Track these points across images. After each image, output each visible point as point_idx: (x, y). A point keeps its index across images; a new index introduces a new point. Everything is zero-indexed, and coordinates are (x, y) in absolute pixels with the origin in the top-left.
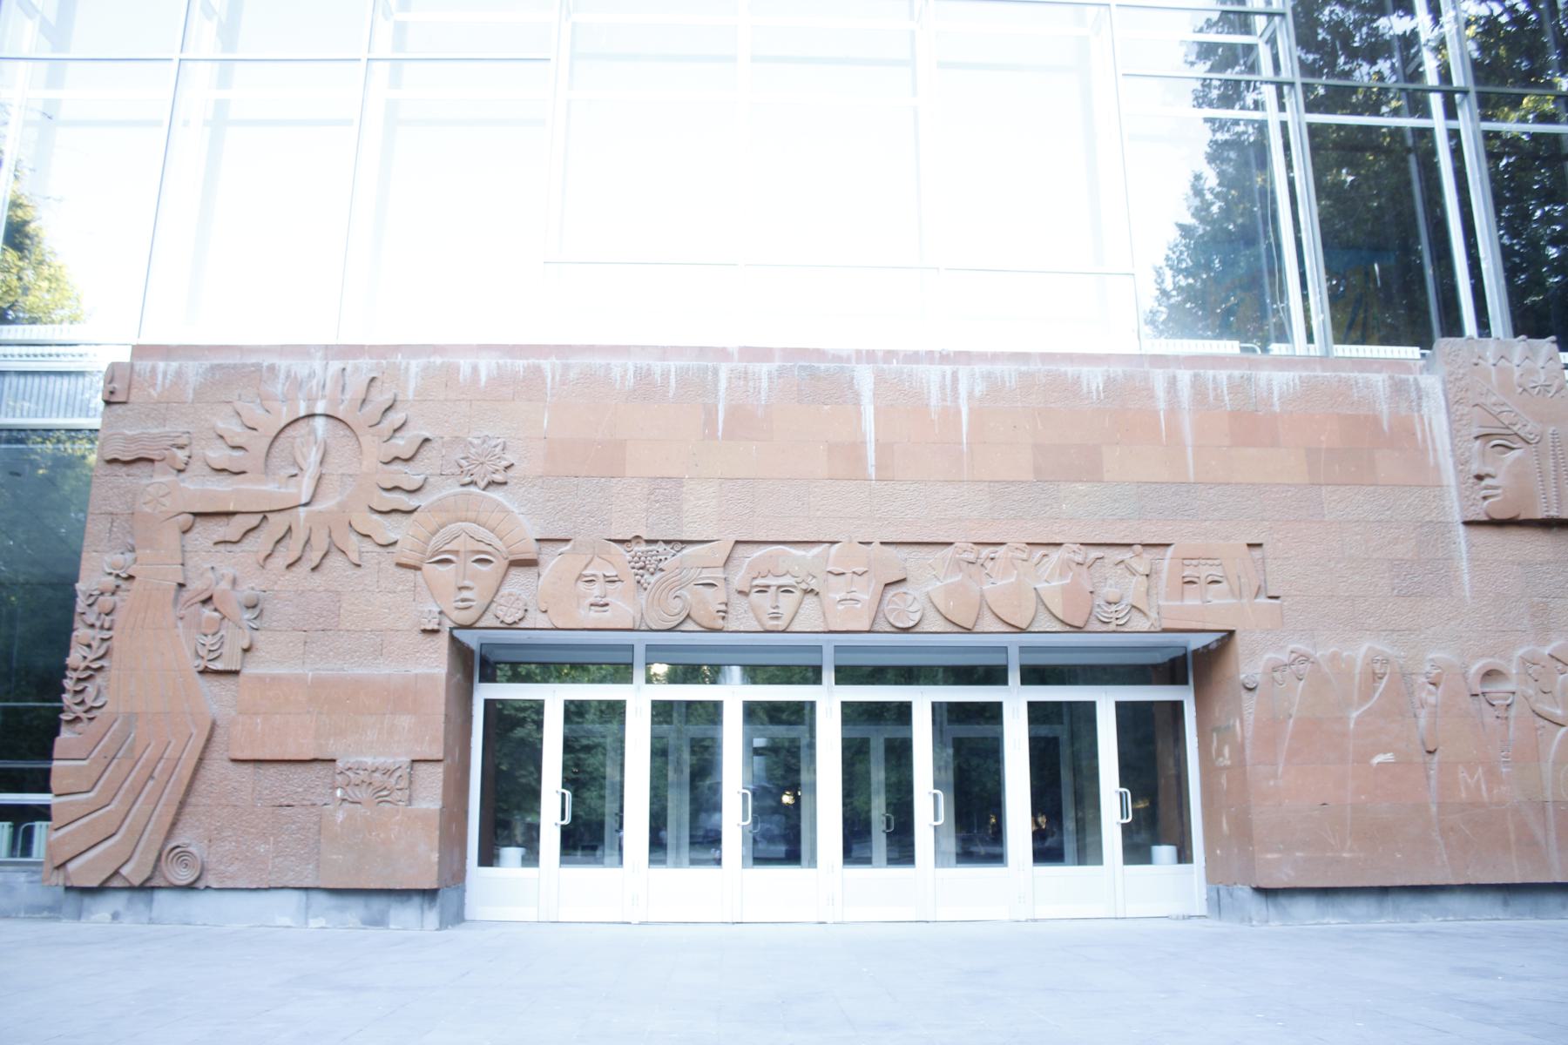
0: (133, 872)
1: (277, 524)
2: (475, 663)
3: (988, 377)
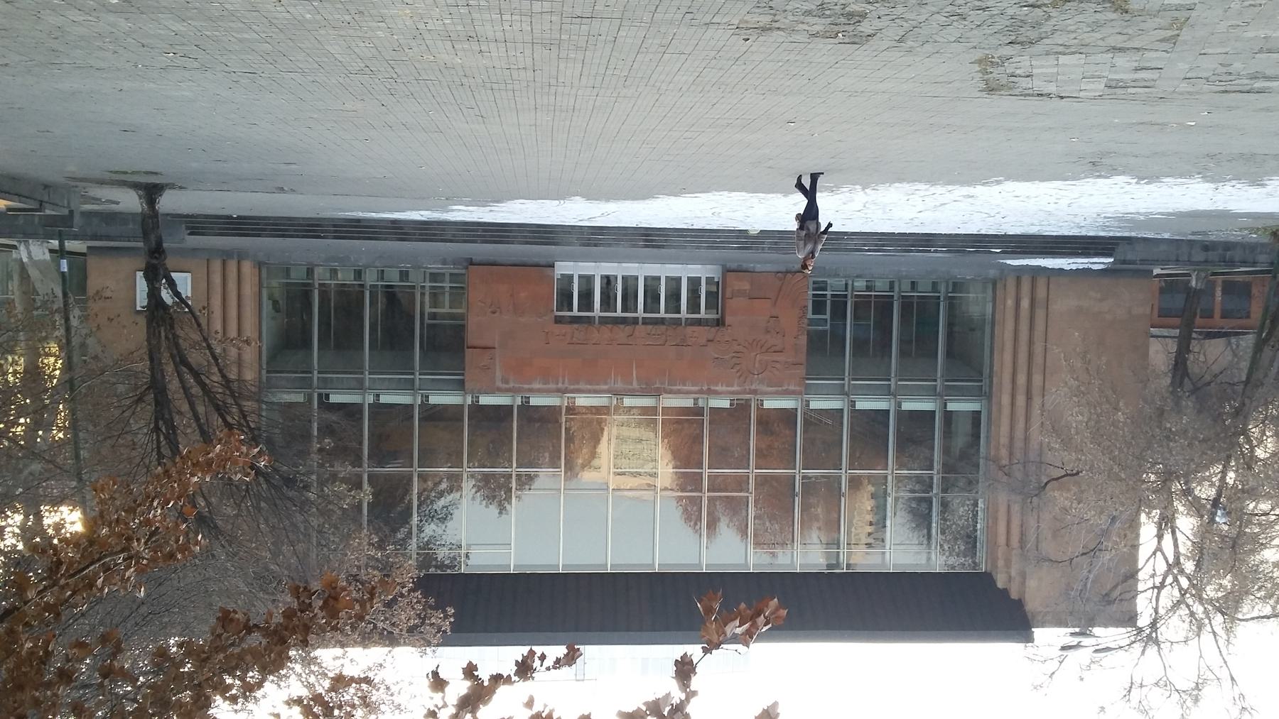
0: (789, 276)
1: (764, 349)
2: (720, 323)
3: (606, 383)
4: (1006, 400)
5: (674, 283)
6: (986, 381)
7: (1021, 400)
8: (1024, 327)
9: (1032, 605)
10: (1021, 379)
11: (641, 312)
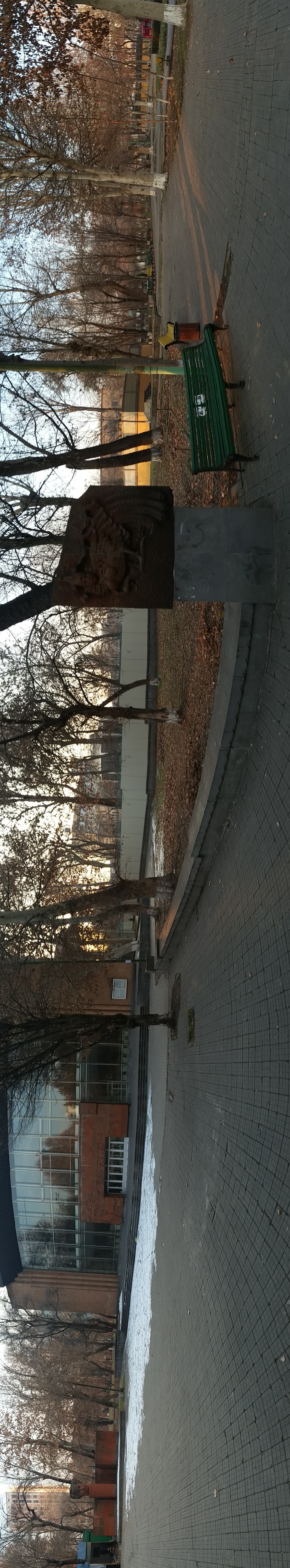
4: (80, 1278)
5: (120, 1178)
6: (85, 1270)
7: (80, 1283)
8: (103, 1284)
9: (14, 1285)
10: (86, 1283)
11: (110, 1173)
